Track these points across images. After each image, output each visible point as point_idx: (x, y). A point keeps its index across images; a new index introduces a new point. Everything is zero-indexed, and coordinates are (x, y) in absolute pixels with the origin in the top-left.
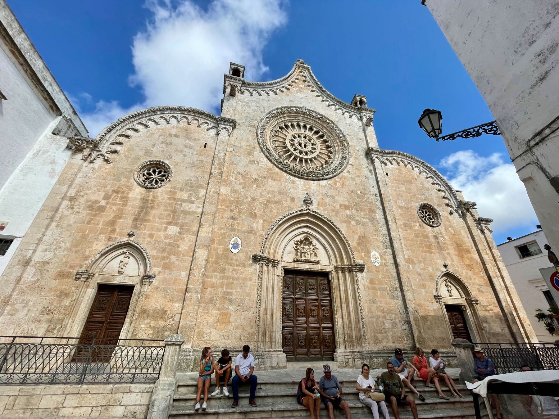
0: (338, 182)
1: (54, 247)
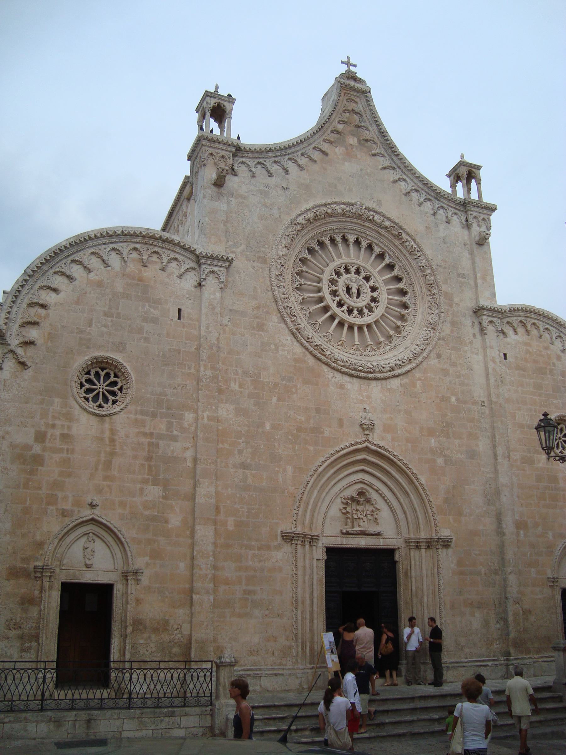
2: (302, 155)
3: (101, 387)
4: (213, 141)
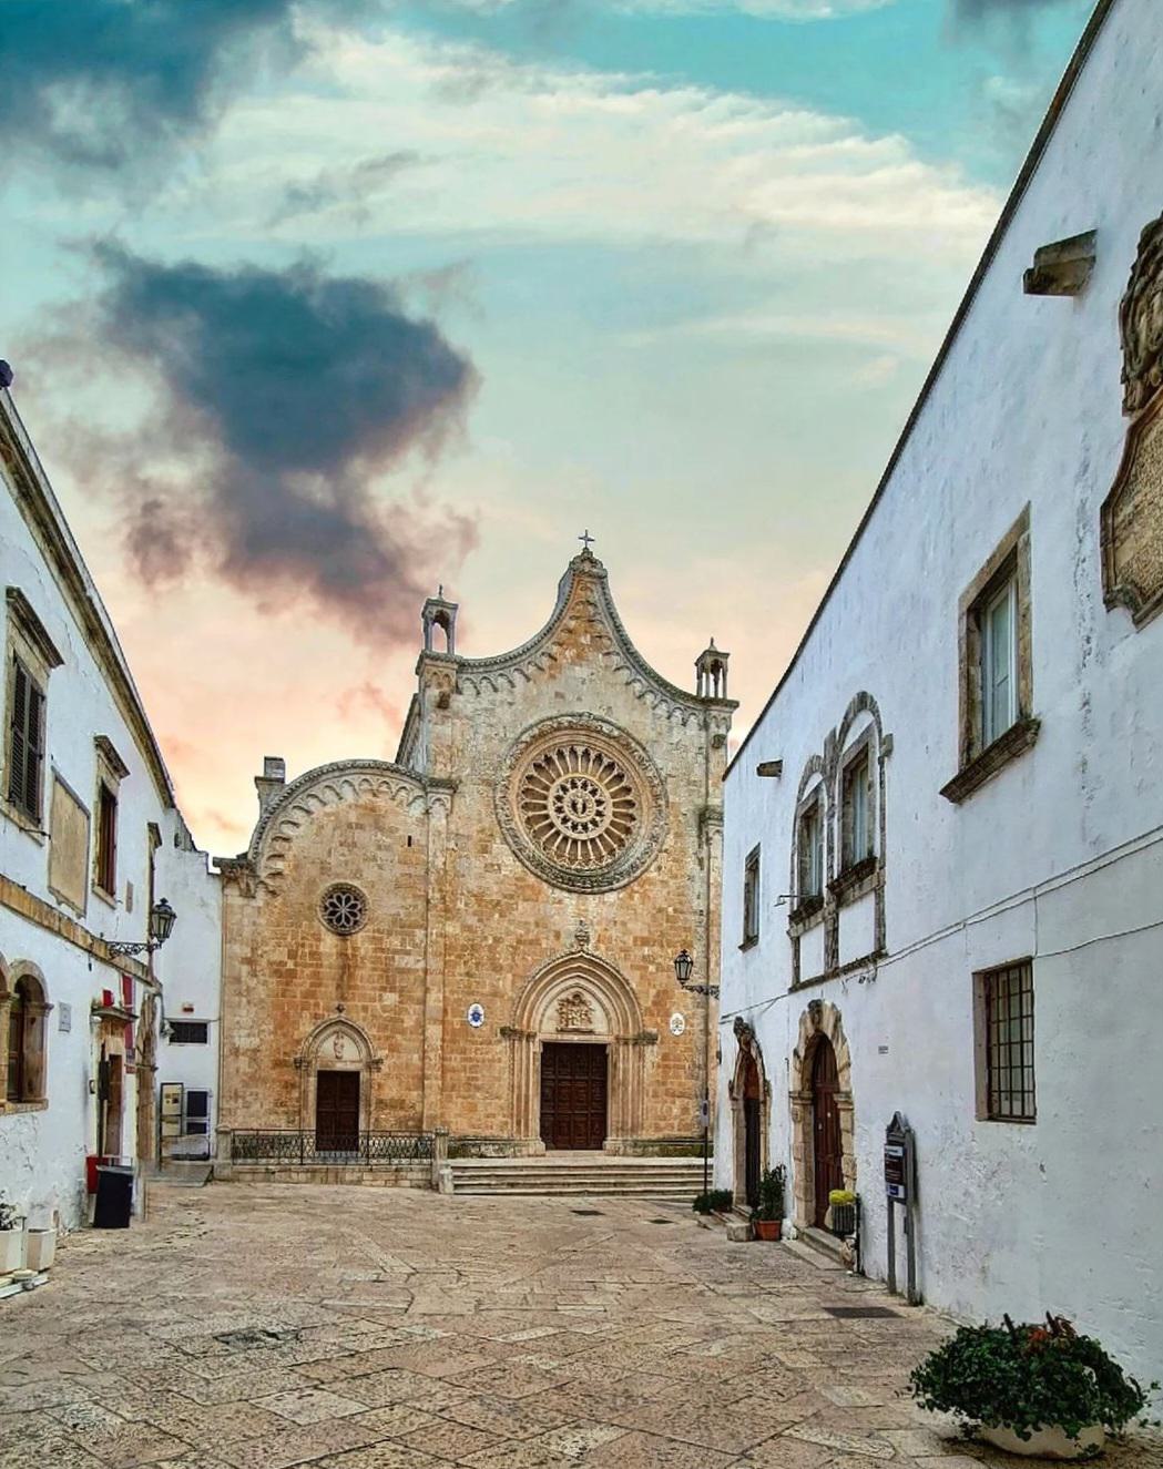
0: (637, 892)
2: (529, 663)
4: (436, 658)
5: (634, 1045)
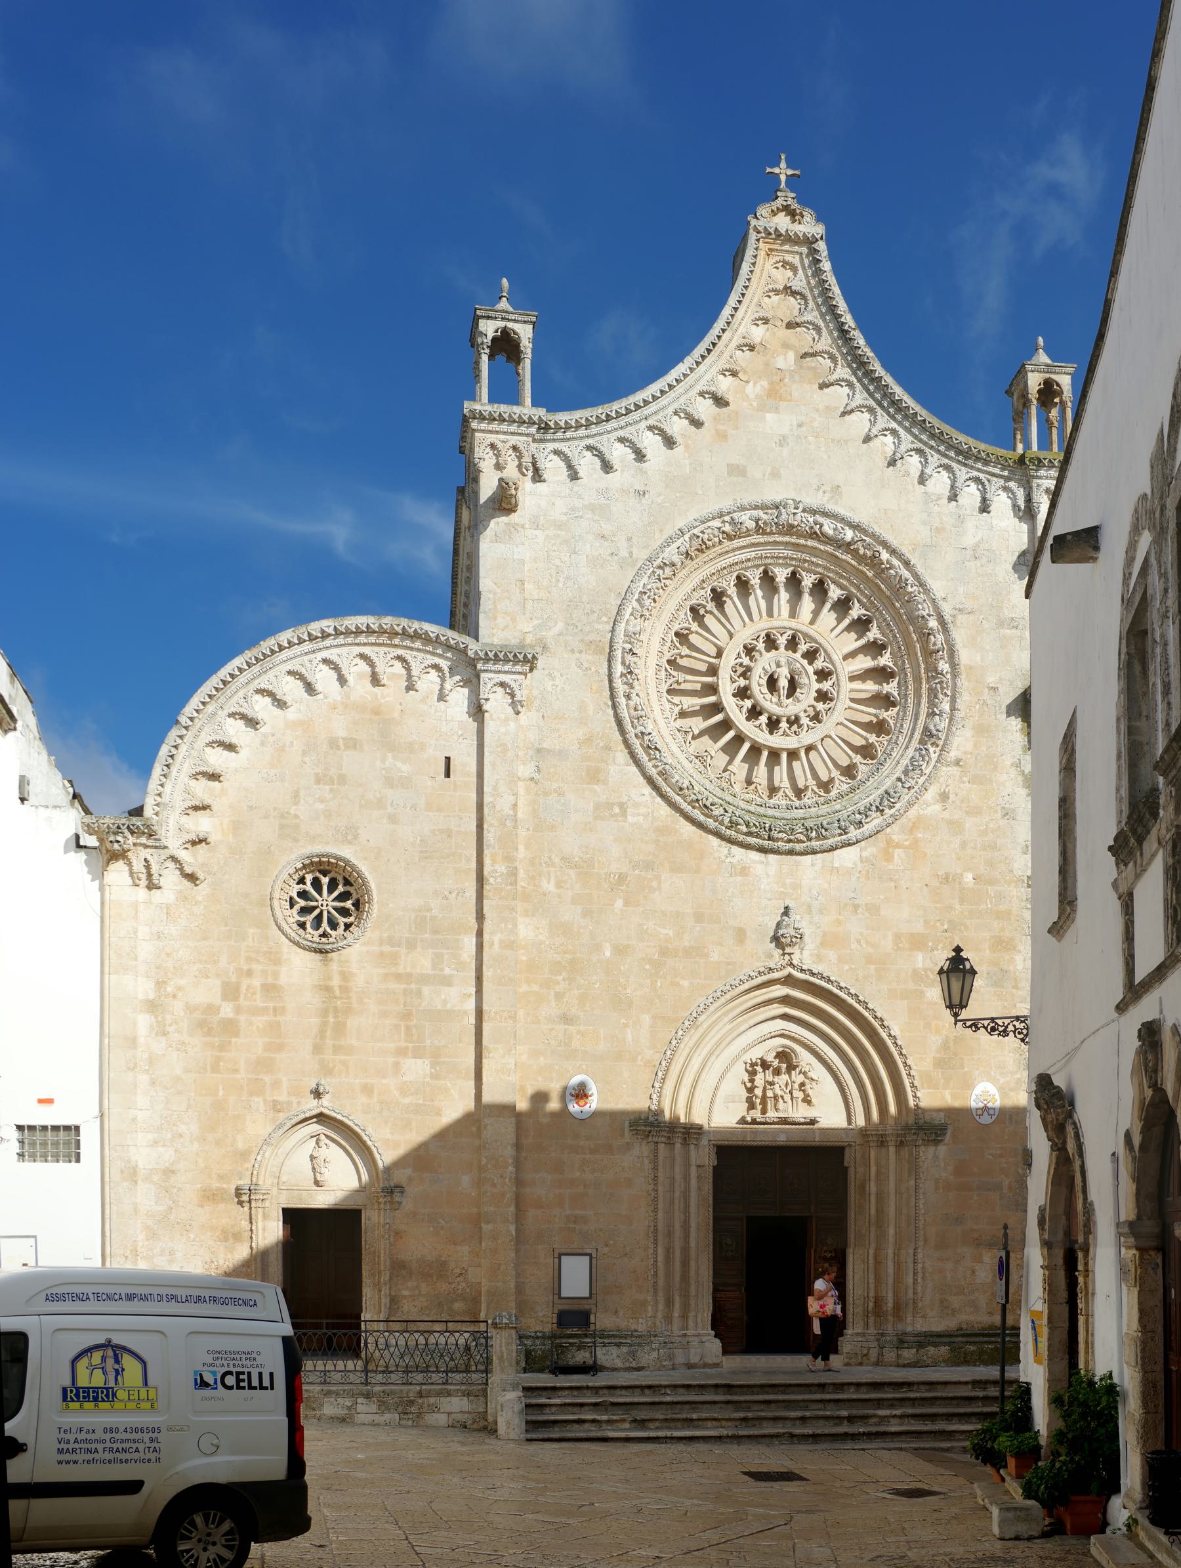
0: (898, 846)
1: (169, 1136)
3: (325, 903)
5: (901, 1144)
